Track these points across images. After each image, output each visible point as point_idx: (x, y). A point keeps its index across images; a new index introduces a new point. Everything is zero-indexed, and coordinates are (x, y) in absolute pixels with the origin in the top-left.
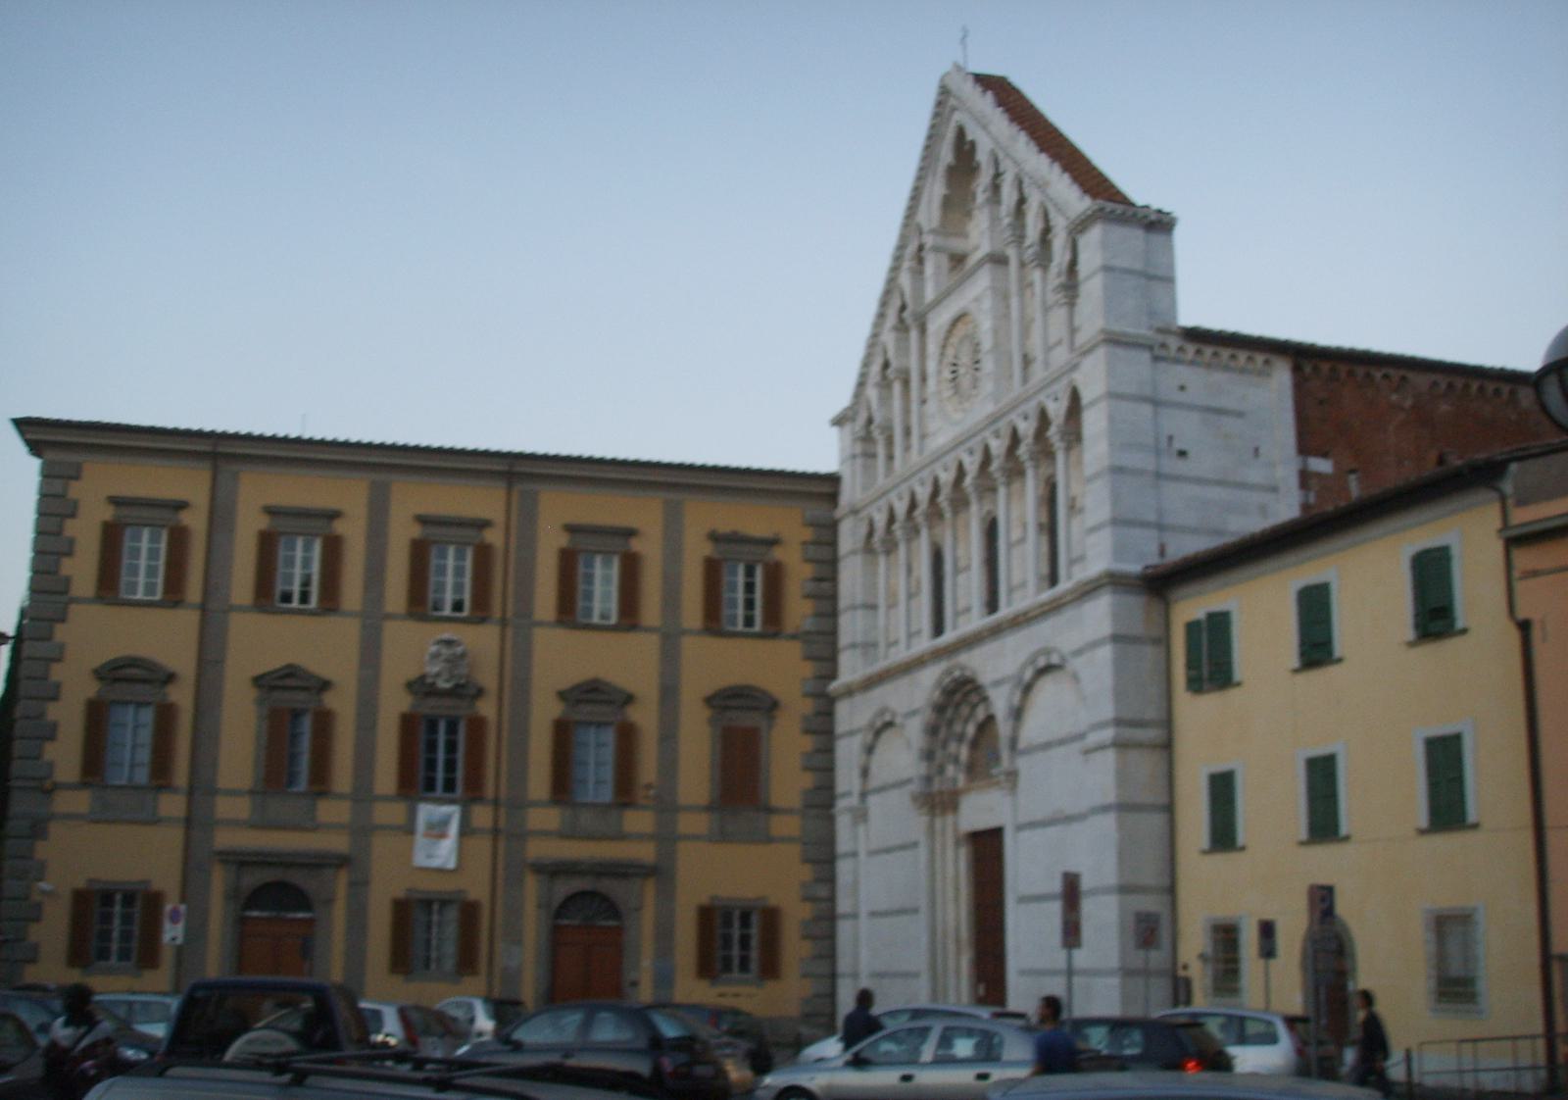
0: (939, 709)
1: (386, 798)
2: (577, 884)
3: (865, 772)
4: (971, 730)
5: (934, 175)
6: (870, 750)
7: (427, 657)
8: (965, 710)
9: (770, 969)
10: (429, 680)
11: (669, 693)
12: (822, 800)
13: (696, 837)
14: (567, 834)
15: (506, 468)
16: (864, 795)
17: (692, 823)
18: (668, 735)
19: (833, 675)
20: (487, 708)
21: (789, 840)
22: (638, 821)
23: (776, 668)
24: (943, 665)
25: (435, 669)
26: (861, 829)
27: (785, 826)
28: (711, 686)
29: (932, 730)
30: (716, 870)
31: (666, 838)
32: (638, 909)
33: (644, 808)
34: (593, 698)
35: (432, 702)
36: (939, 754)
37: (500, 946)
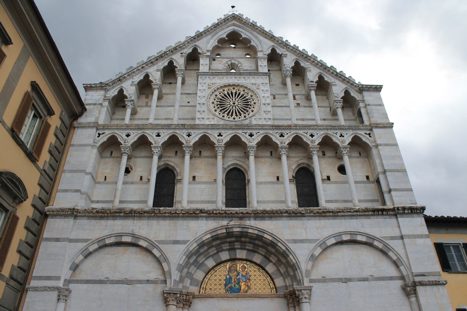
0: (202, 245)
3: (75, 268)
4: (210, 263)
5: (213, 37)
8: (213, 251)
16: (68, 282)
19: (46, 203)
24: (225, 222)
36: (185, 270)
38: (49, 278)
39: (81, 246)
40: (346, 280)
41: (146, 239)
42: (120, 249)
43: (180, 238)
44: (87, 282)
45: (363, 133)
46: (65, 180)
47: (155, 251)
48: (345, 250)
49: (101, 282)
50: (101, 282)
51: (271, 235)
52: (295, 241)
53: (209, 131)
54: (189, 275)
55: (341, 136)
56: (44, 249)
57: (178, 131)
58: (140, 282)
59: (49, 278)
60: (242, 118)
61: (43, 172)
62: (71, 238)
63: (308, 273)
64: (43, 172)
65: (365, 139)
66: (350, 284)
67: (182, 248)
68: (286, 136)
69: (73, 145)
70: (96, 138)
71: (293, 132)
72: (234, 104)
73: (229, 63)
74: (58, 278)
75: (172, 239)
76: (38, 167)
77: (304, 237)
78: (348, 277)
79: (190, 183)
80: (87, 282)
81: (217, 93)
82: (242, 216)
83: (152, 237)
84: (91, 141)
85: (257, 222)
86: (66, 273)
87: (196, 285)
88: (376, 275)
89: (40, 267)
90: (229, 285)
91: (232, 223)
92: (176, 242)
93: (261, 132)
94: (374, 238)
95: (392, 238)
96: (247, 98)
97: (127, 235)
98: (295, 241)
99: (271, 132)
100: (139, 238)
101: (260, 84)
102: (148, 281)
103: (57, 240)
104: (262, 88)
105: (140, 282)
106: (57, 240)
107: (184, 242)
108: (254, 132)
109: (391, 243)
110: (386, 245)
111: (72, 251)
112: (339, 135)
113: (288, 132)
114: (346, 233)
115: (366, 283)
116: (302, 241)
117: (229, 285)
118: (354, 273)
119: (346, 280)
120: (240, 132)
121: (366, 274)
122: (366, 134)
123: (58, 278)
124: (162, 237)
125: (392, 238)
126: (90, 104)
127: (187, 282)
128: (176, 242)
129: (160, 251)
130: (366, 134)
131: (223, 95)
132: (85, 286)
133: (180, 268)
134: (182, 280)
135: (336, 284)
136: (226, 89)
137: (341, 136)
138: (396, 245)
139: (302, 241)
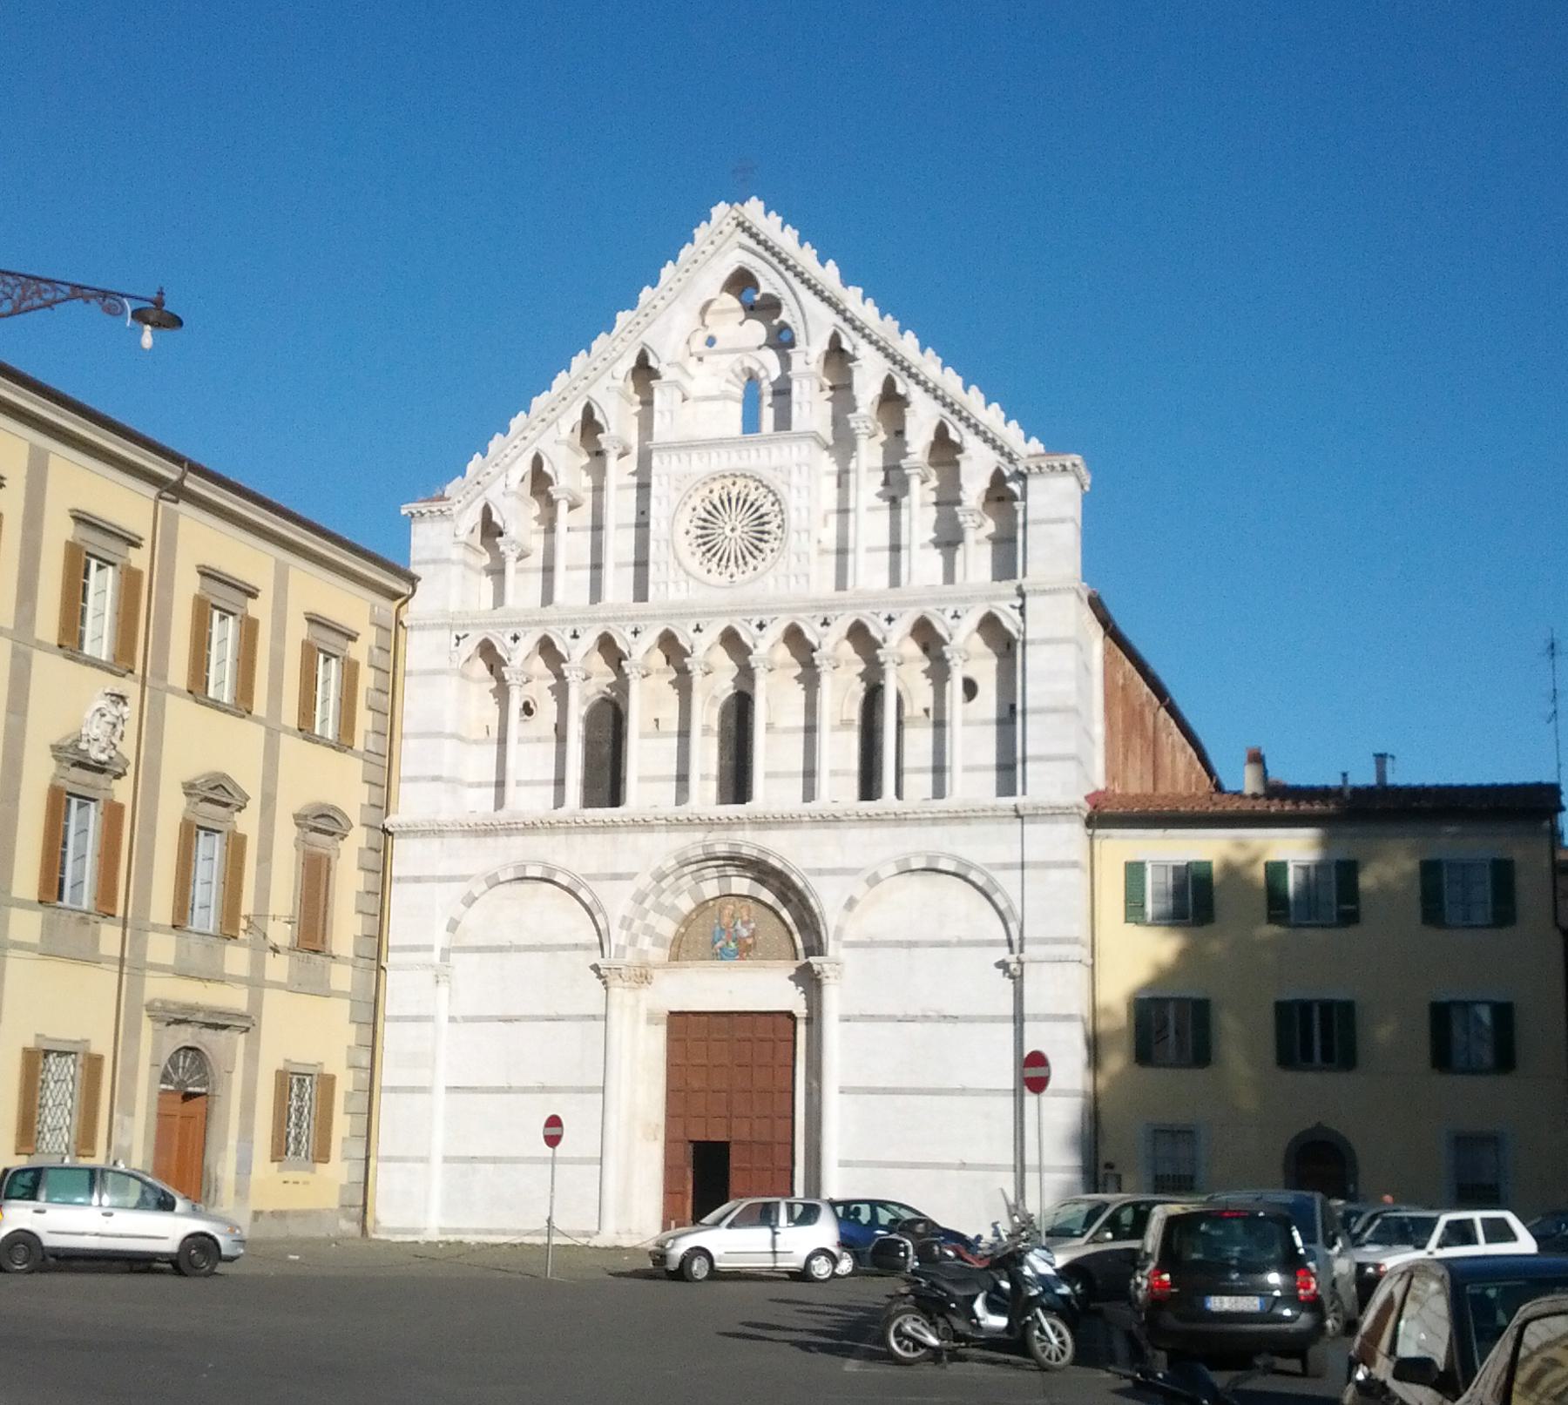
1: (23, 904)
2: (186, 1036)
3: (453, 926)
6: (470, 901)
7: (88, 715)
9: (322, 1155)
10: (83, 746)
11: (269, 800)
12: (374, 952)
13: (278, 985)
14: (182, 973)
15: (174, 477)
16: (446, 953)
17: (278, 967)
18: (265, 857)
19: (385, 807)
20: (122, 791)
21: (341, 994)
22: (236, 959)
23: (339, 782)
24: (699, 836)
25: (95, 732)
26: (443, 990)
27: (342, 977)
28: (298, 805)
29: (640, 898)
30: (302, 1029)
31: (256, 983)
32: (230, 1072)
33: (243, 944)
34: (216, 793)
35: (76, 773)
36: (637, 923)
37: (116, 1116)
38: (415, 949)
39: (460, 889)
40: (912, 944)
41: (566, 872)
42: (526, 887)
43: (620, 870)
44: (479, 949)
45: (1005, 605)
46: (411, 756)
47: (582, 894)
48: (918, 883)
49: (500, 949)
50: (500, 949)
51: (781, 859)
52: (820, 872)
53: (674, 622)
54: (648, 930)
55: (956, 616)
56: (399, 897)
57: (611, 624)
58: (564, 947)
59: (415, 949)
60: (750, 572)
61: (368, 756)
62: (439, 873)
63: (839, 931)
64: (367, 756)
65: (1010, 622)
66: (917, 951)
67: (628, 889)
68: (833, 624)
69: (411, 673)
70: (453, 647)
71: (849, 613)
72: (733, 530)
73: (738, 369)
74: (430, 948)
75: (609, 870)
76: (357, 754)
77: (838, 862)
78: (914, 938)
79: (643, 736)
80: (479, 949)
81: (696, 501)
82: (730, 824)
83: (574, 868)
84: (440, 662)
85: (756, 833)
86: (440, 938)
87: (663, 946)
88: (966, 936)
89: (398, 931)
90: (719, 944)
91: (712, 836)
92: (616, 877)
93: (782, 616)
94: (970, 867)
95: (1006, 867)
96: (762, 511)
97: (535, 863)
98: (820, 872)
99: (802, 615)
100: (553, 870)
101: (795, 470)
102: (576, 946)
103: (417, 880)
104: (795, 479)
105: (564, 947)
106: (417, 880)
107: (630, 876)
108: (766, 619)
109: (1001, 877)
110: (991, 880)
111: (446, 897)
112: (950, 613)
113: (837, 613)
114: (918, 854)
115: (944, 950)
116: (833, 872)
117: (719, 944)
118: (927, 932)
119: (912, 944)
120: (739, 619)
121: (949, 934)
122: (1013, 607)
123: (430, 948)
124: (593, 870)
125: (1006, 867)
126: (427, 562)
127: (645, 942)
128: (616, 877)
129: (591, 892)
130: (1013, 607)
131: (710, 508)
132: (476, 957)
133: (626, 923)
134: (633, 941)
135: (889, 951)
136: (717, 486)
137: (956, 616)
138: (1008, 883)
139: (833, 872)
